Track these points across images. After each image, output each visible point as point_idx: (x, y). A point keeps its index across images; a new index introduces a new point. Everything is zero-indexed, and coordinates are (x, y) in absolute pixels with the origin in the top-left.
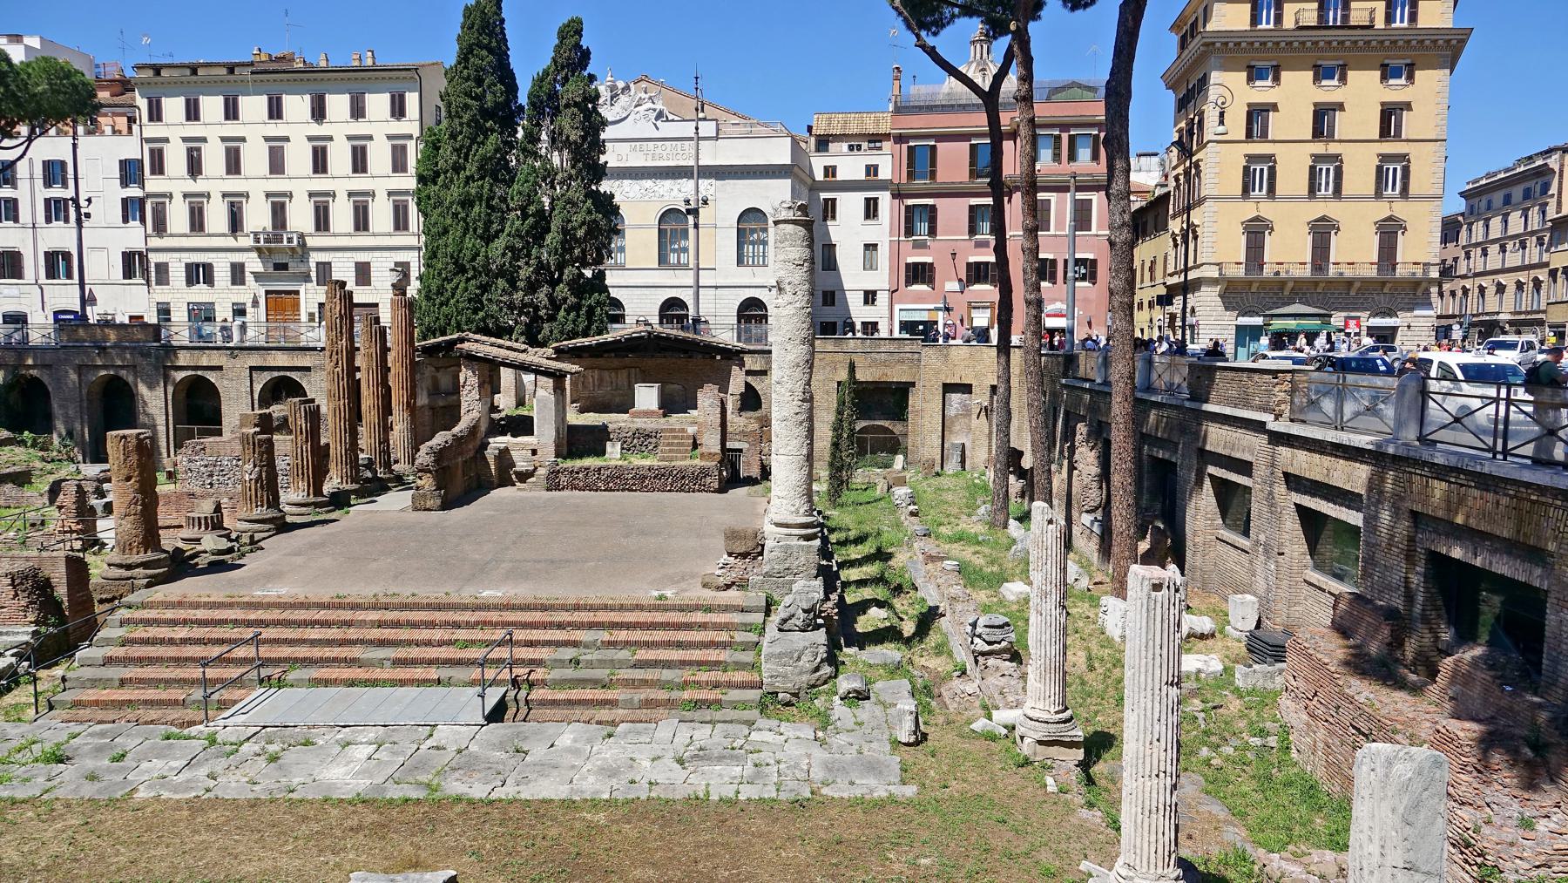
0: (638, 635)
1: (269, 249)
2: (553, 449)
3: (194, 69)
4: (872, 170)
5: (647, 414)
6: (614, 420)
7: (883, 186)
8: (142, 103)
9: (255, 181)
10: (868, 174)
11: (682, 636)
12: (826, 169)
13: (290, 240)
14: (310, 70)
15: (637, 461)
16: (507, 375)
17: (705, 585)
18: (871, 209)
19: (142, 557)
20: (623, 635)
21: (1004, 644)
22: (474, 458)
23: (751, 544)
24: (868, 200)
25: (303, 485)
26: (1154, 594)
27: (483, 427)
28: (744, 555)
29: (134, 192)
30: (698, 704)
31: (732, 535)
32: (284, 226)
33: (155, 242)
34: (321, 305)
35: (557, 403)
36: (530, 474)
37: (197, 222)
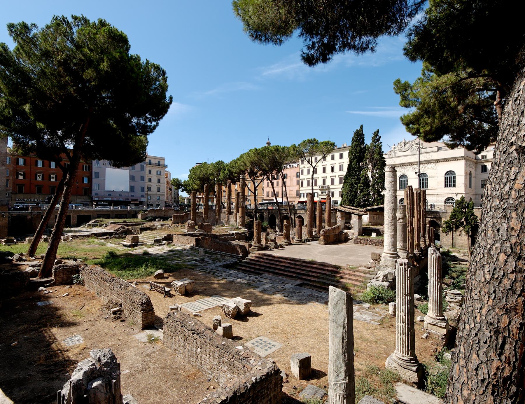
2: (357, 233)
16: (352, 215)
17: (365, 267)
19: (256, 245)
21: (456, 300)
23: (378, 257)
25: (298, 236)
27: (342, 227)
28: (376, 260)
31: (373, 254)
35: (359, 222)
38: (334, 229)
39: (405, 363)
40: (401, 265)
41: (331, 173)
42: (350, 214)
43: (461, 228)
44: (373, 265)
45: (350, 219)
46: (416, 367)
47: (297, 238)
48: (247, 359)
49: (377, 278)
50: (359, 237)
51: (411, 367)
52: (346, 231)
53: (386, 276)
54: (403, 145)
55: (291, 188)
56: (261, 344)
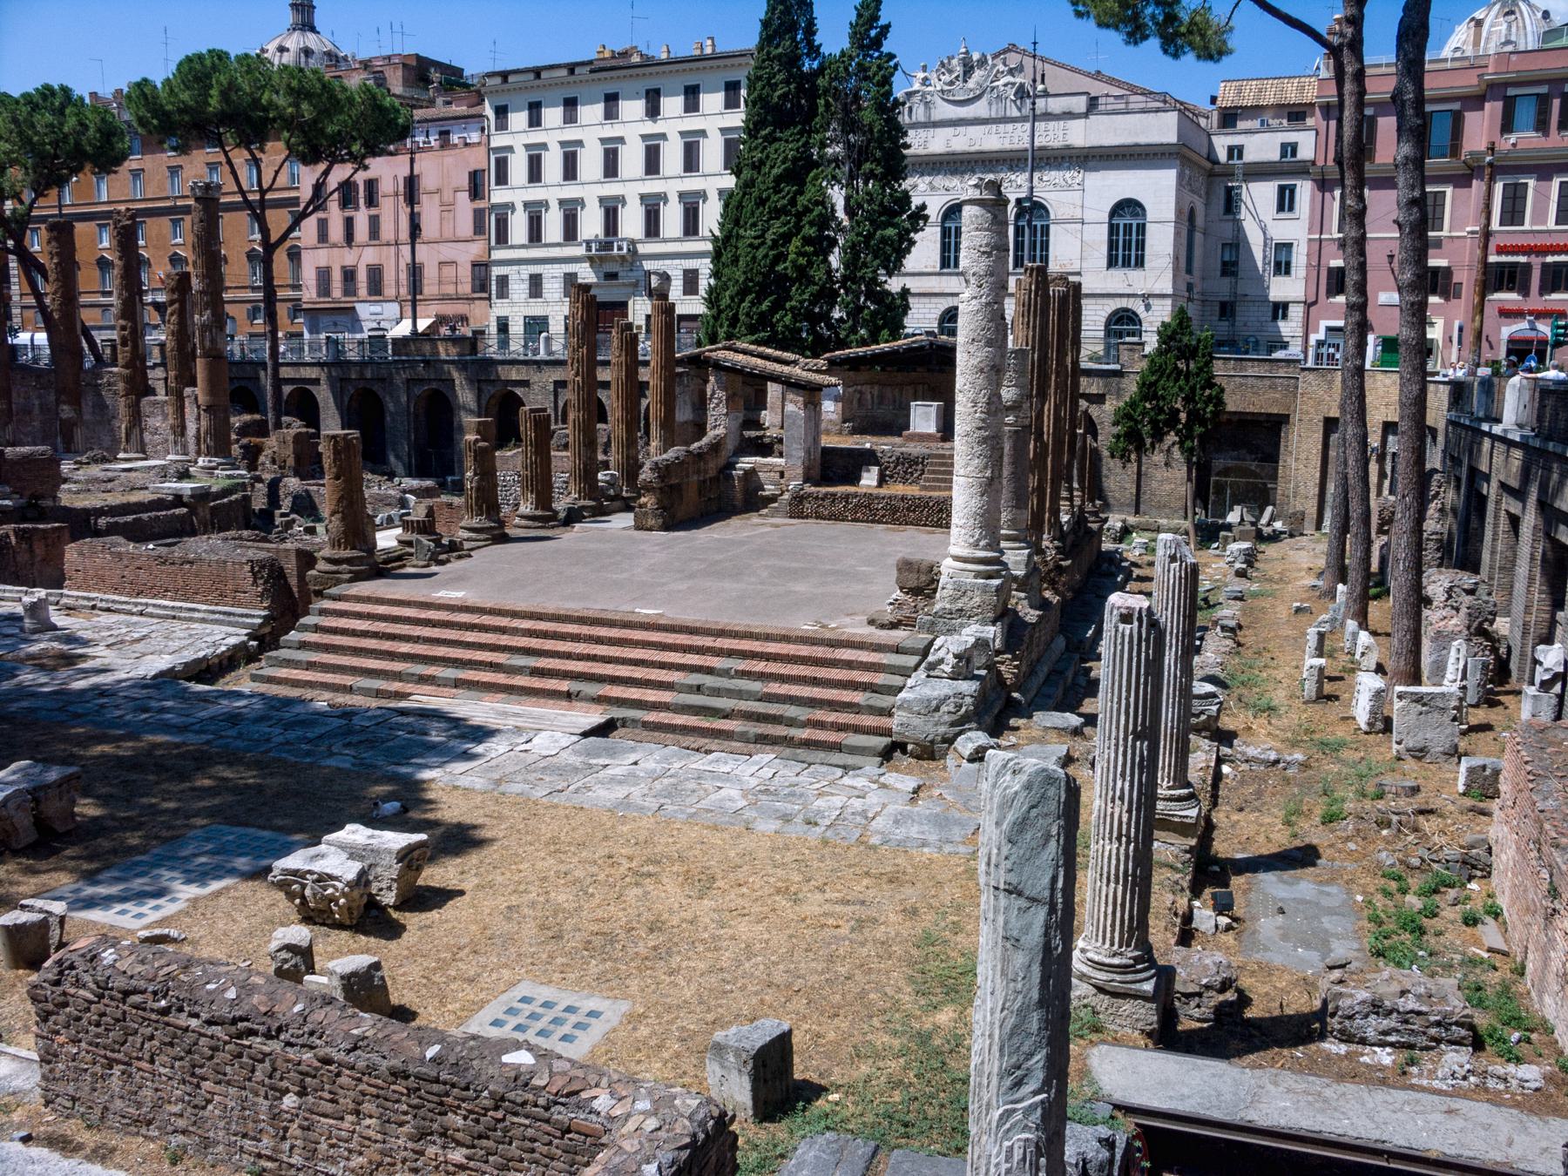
0: (773, 668)
1: (601, 258)
2: (800, 471)
3: (537, 72)
4: (1289, 149)
5: (923, 438)
6: (884, 445)
7: (1303, 170)
8: (489, 111)
9: (591, 187)
10: (1283, 155)
11: (822, 673)
12: (1231, 149)
13: (620, 248)
14: (649, 63)
15: (897, 489)
16: (773, 390)
17: (871, 622)
18: (1286, 201)
19: (348, 553)
20: (760, 666)
21: (1203, 717)
22: (715, 480)
24: (1282, 189)
25: (531, 497)
26: (1121, 626)
27: (730, 445)
28: (915, 591)
29: (481, 204)
30: (807, 744)
31: (906, 566)
32: (615, 233)
33: (498, 255)
34: (648, 317)
35: (807, 419)
36: (773, 499)
37: (535, 235)
38: (700, 456)
39: (1118, 977)
40: (1126, 618)
41: (659, 181)
42: (757, 382)
43: (1172, 438)
44: (906, 612)
45: (760, 402)
46: (1153, 981)
47: (526, 508)
48: (573, 1100)
49: (932, 667)
50: (809, 489)
51: (1137, 986)
52: (746, 462)
53: (964, 658)
54: (959, 70)
55: (448, 252)
56: (534, 1016)
